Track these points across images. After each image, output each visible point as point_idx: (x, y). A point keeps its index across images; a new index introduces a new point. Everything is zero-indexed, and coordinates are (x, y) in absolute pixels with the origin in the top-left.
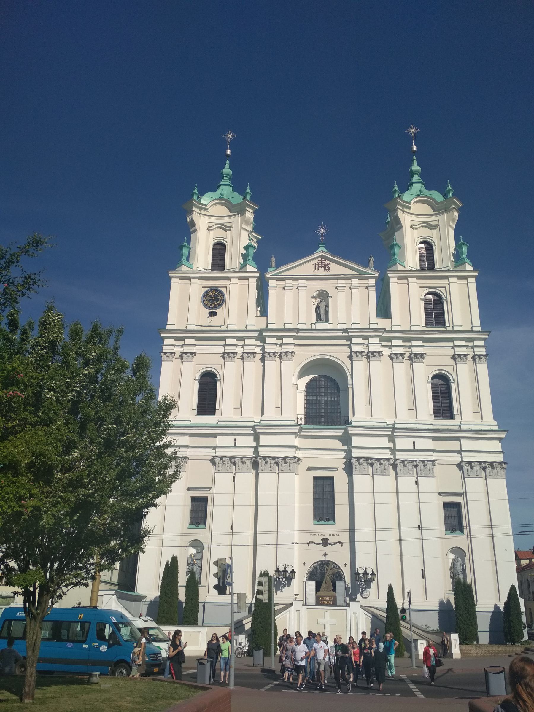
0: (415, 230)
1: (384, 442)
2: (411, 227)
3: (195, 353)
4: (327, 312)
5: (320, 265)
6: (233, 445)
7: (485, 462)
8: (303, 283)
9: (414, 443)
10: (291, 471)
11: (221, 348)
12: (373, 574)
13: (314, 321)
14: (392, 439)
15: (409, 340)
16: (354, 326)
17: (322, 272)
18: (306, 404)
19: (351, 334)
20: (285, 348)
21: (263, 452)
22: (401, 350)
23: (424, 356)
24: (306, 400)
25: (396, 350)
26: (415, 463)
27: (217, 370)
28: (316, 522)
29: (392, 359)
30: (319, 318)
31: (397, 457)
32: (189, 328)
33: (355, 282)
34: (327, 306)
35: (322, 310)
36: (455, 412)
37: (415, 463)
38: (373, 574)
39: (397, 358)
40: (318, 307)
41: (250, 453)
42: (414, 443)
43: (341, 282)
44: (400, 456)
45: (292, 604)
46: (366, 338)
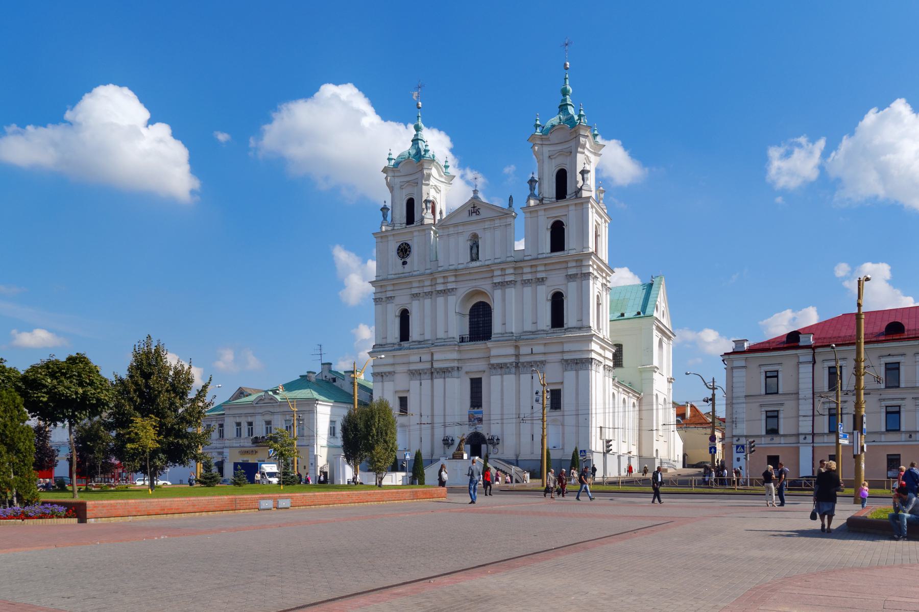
0: (553, 160)
1: (511, 351)
2: (549, 157)
3: (394, 297)
4: (478, 251)
5: (473, 211)
6: (419, 361)
7: (577, 359)
8: (461, 229)
9: (532, 349)
10: (452, 377)
11: (409, 290)
12: (498, 439)
13: (469, 260)
14: (517, 347)
15: (536, 266)
16: (497, 261)
17: (474, 217)
18: (470, 325)
19: (492, 268)
20: (450, 286)
21: (436, 365)
22: (529, 277)
23: (544, 279)
24: (471, 322)
25: (526, 277)
26: (531, 364)
27: (408, 307)
28: (472, 408)
29: (522, 284)
30: (472, 260)
31: (520, 361)
32: (390, 277)
33: (497, 223)
34: (478, 247)
35: (474, 251)
36: (565, 322)
37: (531, 364)
38: (498, 439)
39: (526, 283)
40: (471, 248)
41: (428, 366)
42: (532, 349)
43: (487, 224)
44: (522, 359)
45: (439, 460)
46: (502, 269)
